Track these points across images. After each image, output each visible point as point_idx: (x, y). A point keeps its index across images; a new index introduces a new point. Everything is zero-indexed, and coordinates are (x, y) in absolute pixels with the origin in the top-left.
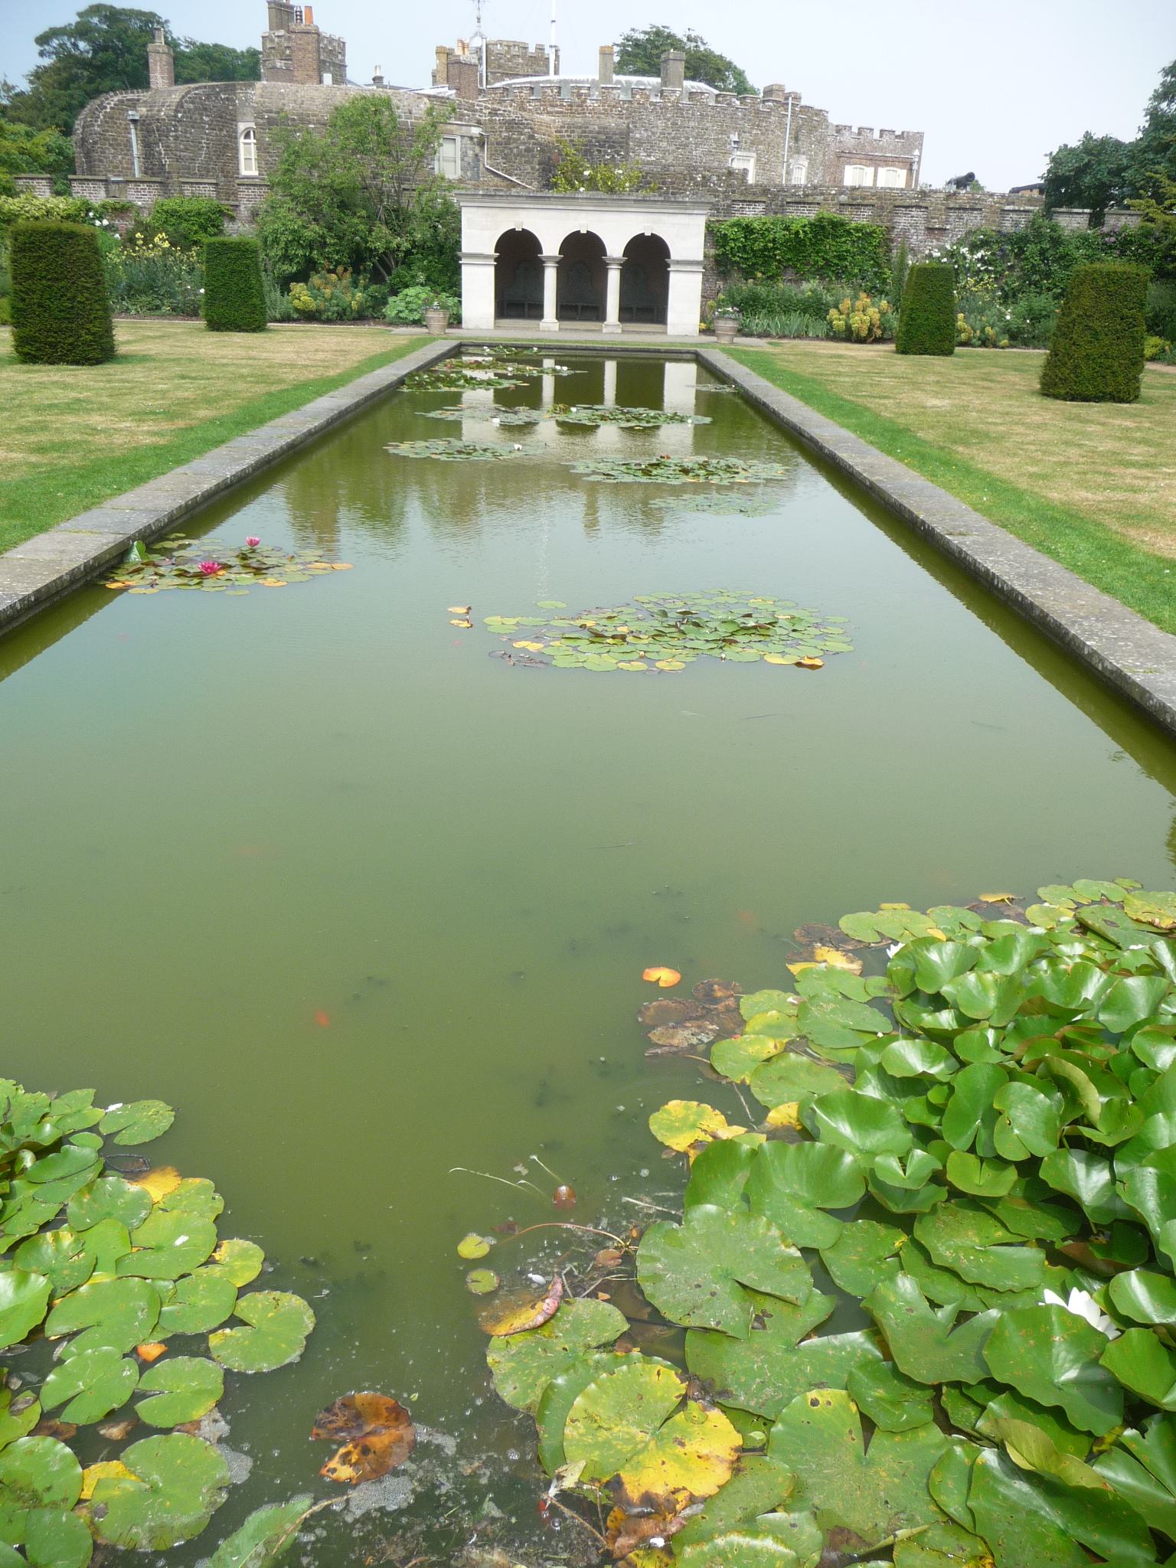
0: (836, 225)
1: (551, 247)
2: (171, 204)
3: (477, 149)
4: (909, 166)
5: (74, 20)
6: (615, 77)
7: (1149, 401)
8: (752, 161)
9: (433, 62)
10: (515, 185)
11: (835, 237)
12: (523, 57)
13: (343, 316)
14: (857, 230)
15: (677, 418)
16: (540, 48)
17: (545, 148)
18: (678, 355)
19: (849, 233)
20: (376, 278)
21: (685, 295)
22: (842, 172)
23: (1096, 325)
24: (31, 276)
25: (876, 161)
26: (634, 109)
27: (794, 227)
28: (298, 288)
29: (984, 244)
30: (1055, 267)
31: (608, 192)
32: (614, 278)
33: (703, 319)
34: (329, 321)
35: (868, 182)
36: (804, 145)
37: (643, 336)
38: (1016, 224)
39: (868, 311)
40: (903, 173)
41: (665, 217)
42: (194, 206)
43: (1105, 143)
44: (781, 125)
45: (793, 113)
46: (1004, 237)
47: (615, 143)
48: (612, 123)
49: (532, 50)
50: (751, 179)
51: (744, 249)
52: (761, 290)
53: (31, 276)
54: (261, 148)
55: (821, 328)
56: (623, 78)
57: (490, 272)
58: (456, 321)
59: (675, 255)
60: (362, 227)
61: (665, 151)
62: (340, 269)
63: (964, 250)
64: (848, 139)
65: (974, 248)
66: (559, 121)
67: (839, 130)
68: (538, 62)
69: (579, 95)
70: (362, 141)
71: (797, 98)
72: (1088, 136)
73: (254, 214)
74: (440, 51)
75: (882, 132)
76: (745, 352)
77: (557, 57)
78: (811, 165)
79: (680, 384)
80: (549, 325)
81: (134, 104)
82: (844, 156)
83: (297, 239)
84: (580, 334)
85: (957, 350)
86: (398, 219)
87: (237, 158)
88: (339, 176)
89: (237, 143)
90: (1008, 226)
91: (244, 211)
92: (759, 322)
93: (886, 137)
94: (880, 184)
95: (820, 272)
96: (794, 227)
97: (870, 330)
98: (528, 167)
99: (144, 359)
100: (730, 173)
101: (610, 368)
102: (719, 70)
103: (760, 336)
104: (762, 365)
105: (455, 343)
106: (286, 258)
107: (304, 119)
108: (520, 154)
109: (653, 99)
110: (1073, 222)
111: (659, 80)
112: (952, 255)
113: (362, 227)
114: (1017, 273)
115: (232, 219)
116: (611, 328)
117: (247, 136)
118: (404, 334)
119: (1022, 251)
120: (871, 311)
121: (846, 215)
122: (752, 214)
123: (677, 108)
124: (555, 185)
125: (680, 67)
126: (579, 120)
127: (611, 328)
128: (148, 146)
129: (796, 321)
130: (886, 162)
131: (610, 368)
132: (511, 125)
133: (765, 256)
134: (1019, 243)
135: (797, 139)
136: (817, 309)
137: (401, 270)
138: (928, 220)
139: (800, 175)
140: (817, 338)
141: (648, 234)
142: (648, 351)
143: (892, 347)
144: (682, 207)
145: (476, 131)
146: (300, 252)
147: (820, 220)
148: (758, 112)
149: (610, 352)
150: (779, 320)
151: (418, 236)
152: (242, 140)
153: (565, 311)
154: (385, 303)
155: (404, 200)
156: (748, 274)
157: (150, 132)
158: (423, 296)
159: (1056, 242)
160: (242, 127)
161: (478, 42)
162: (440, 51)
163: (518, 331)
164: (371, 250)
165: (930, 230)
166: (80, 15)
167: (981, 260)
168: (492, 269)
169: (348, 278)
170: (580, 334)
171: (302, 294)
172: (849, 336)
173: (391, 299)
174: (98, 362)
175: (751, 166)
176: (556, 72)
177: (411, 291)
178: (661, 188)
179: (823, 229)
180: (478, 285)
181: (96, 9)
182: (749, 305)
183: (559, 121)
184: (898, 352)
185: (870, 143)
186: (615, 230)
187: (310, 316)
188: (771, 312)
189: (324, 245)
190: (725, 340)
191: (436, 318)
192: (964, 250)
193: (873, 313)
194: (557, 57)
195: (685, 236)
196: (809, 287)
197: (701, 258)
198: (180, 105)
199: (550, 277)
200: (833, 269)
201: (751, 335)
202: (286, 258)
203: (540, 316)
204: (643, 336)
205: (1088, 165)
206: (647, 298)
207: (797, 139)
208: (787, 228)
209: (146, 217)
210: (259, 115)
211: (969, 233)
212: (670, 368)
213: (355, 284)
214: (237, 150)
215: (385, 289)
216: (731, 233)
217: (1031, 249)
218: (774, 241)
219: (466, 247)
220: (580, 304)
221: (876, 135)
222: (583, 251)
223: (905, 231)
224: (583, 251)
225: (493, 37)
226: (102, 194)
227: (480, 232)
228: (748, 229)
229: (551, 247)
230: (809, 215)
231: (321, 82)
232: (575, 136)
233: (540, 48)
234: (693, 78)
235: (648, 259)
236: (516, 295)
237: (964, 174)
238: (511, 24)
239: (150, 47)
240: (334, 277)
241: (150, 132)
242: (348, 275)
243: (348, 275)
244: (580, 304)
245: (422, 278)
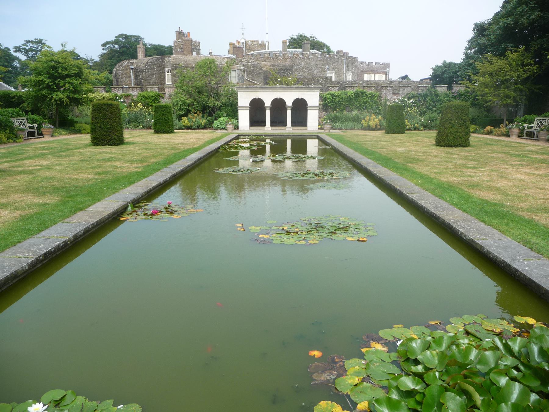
0: (362, 93)
1: (268, 103)
2: (143, 94)
3: (243, 73)
4: (386, 73)
5: (114, 39)
6: (288, 50)
7: (473, 146)
8: (333, 74)
9: (228, 47)
10: (255, 84)
11: (362, 97)
12: (257, 45)
13: (199, 127)
14: (370, 94)
15: (312, 158)
16: (263, 42)
17: (265, 72)
18: (311, 137)
19: (367, 95)
20: (210, 115)
21: (313, 118)
22: (363, 76)
23: (453, 122)
24: (98, 118)
25: (374, 73)
26: (294, 59)
27: (348, 94)
28: (184, 119)
29: (413, 97)
30: (437, 104)
31: (287, 85)
32: (289, 112)
33: (319, 124)
34: (194, 129)
35: (372, 79)
36: (350, 68)
37: (299, 131)
38: (423, 91)
39: (375, 120)
40: (384, 76)
41: (305, 93)
42: (151, 94)
43: (450, 64)
44: (343, 63)
45: (346, 58)
46: (419, 95)
47: (288, 70)
48: (287, 64)
49: (260, 42)
50: (333, 79)
51: (332, 102)
52: (339, 115)
53: (98, 118)
55: (359, 126)
56: (290, 50)
57: (247, 112)
58: (237, 128)
59: (309, 104)
60: (205, 99)
61: (304, 72)
62: (198, 112)
63: (406, 99)
64: (365, 66)
65: (409, 99)
66: (269, 64)
67: (362, 63)
68: (262, 46)
69: (276, 56)
70: (205, 72)
71: (347, 54)
72: (445, 62)
73: (170, 96)
74: (230, 44)
75: (376, 63)
76: (334, 135)
77: (268, 44)
78: (353, 74)
79: (312, 146)
80: (268, 128)
81: (132, 64)
82: (364, 71)
83: (184, 103)
84: (278, 131)
85: (406, 132)
86: (217, 96)
87: (165, 79)
88: (198, 83)
89: (165, 74)
90: (420, 91)
91: (167, 95)
92: (338, 125)
93: (377, 65)
94: (376, 79)
95: (358, 108)
96: (348, 94)
97: (376, 126)
98: (260, 78)
99: (133, 143)
100: (326, 78)
101: (289, 142)
102: (321, 46)
103: (339, 129)
104: (339, 139)
105: (236, 135)
106: (180, 109)
107: (187, 66)
108: (257, 74)
109: (300, 56)
110: (442, 89)
111: (301, 50)
112: (402, 101)
113: (205, 99)
114: (424, 106)
115: (163, 98)
116: (289, 129)
117: (168, 72)
118: (219, 133)
119: (425, 99)
120: (376, 120)
121: (366, 90)
122: (334, 90)
123: (308, 59)
124: (269, 83)
125: (309, 46)
126: (276, 63)
128: (136, 76)
129: (350, 124)
130: (378, 73)
131: (289, 142)
132: (254, 66)
133: (339, 104)
134: (424, 96)
135: (348, 66)
136: (357, 120)
137: (218, 112)
138: (393, 90)
139: (350, 77)
140: (358, 129)
141: (300, 98)
142: (301, 135)
143: (384, 131)
144: (311, 89)
145: (242, 68)
146: (185, 107)
147: (357, 91)
148: (335, 59)
149: (288, 136)
150: (345, 124)
151: (224, 101)
152: (167, 73)
153: (273, 124)
154: (213, 123)
155: (219, 90)
156: (334, 109)
157: (137, 72)
158: (226, 120)
159: (437, 96)
160: (167, 69)
161: (242, 41)
162: (231, 44)
163: (257, 130)
164: (208, 106)
165: (394, 93)
166: (116, 37)
167: (412, 102)
168: (248, 111)
169: (201, 115)
170: (278, 131)
171: (185, 121)
172: (369, 128)
173: (215, 121)
174: (118, 145)
175: (333, 75)
176: (268, 49)
177: (222, 119)
178: (305, 83)
179: (358, 95)
180: (244, 117)
181: (121, 35)
182: (334, 120)
183: (269, 64)
184: (386, 133)
185: (372, 67)
187: (188, 128)
188: (342, 122)
189: (193, 105)
190: (327, 131)
191: (230, 127)
192: (406, 99)
193: (377, 120)
194: (268, 44)
195: (312, 98)
196: (355, 113)
197: (318, 105)
198: (147, 63)
200: (362, 107)
201: (336, 129)
202: (180, 109)
204: (299, 131)
205: (445, 71)
206: (300, 118)
207: (348, 66)
208: (346, 95)
209: (135, 98)
210: (172, 65)
211: (407, 94)
212: (309, 141)
213: (203, 117)
214: (165, 76)
215: (213, 118)
216: (328, 96)
217: (429, 98)
218: (342, 99)
219: (239, 105)
220: (278, 120)
221: (374, 64)
222: (279, 105)
223: (386, 94)
224: (279, 105)
225: (247, 39)
226: (121, 91)
227: (244, 99)
228: (333, 95)
229: (268, 103)
230: (354, 90)
231: (192, 55)
232: (275, 68)
234: (313, 49)
235: (300, 106)
236: (257, 119)
237: (404, 75)
238: (253, 34)
239: (138, 46)
240: (196, 115)
241: (137, 72)
242: (201, 114)
243: (201, 114)
244: (278, 120)
245: (225, 114)
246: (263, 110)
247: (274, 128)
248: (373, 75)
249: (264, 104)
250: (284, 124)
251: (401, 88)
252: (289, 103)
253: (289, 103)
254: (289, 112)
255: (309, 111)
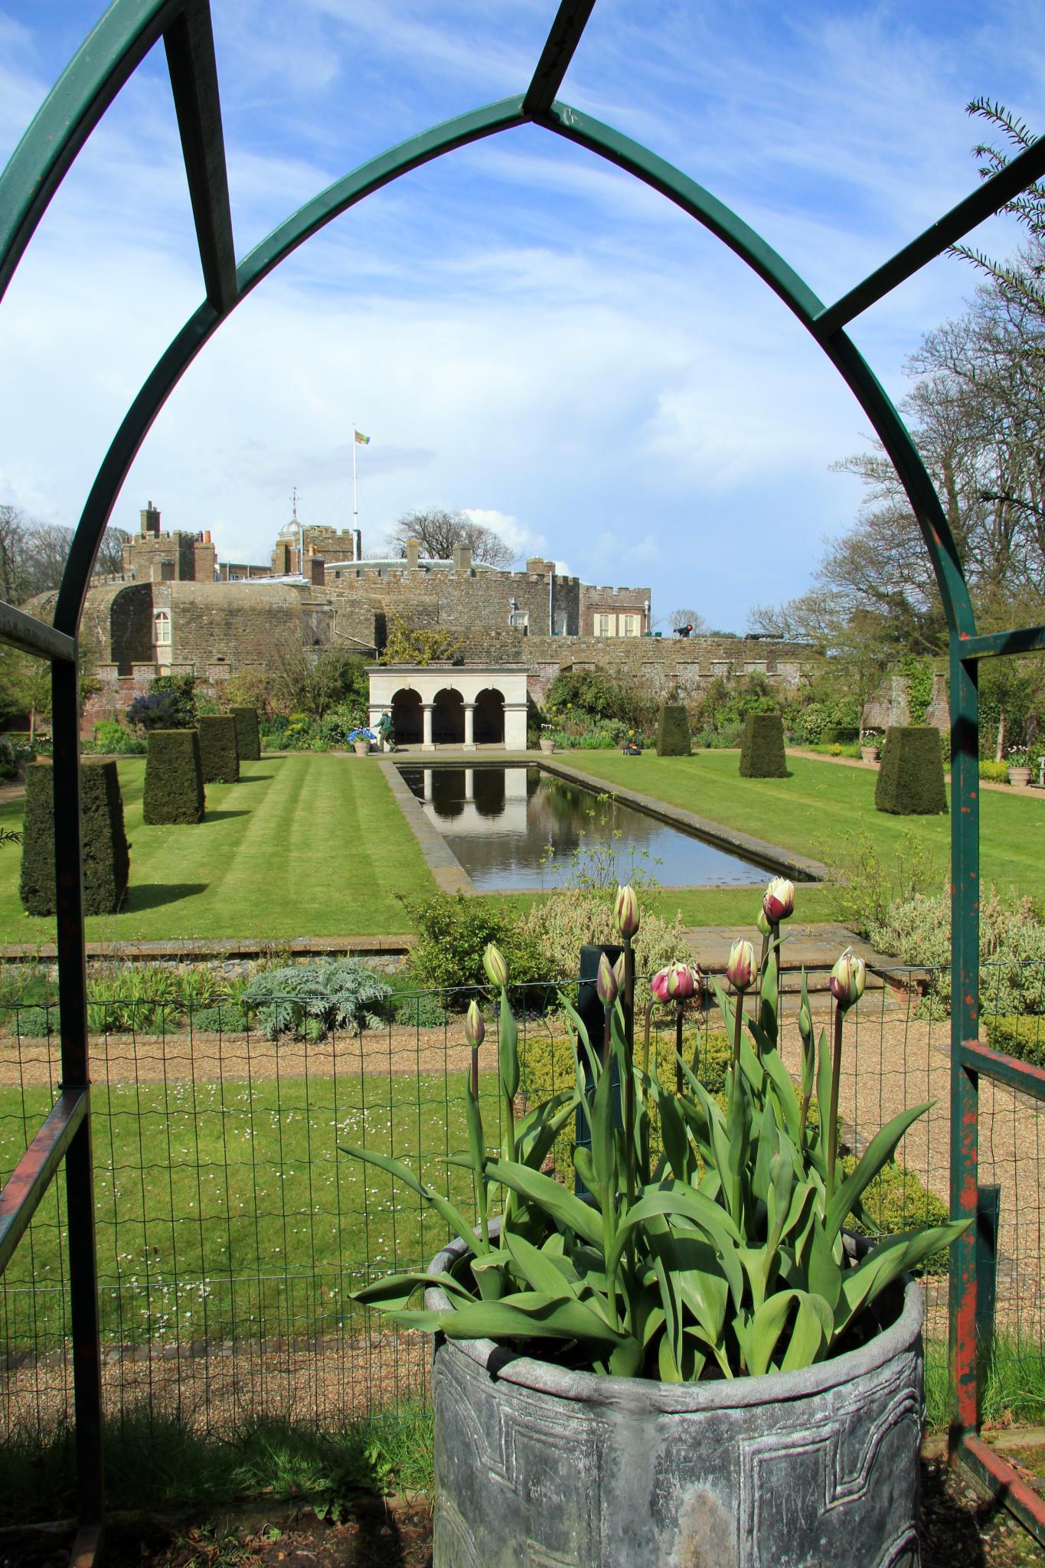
12: (332, 538)
16: (346, 532)
21: (515, 724)
25: (616, 610)
32: (469, 716)
37: (489, 752)
40: (637, 619)
49: (339, 533)
54: (176, 627)
59: (507, 701)
67: (588, 589)
79: (515, 782)
80: (427, 748)
82: (593, 607)
84: (450, 752)
101: (469, 774)
107: (209, 608)
108: (360, 622)
116: (468, 748)
127: (468, 748)
131: (469, 774)
153: (437, 738)
160: (155, 611)
161: (294, 528)
170: (450, 752)
186: (470, 687)
199: (427, 716)
203: (422, 741)
204: (489, 752)
206: (490, 728)
210: (174, 607)
212: (508, 771)
219: (372, 701)
220: (448, 732)
221: (615, 589)
222: (449, 700)
224: (449, 700)
225: (307, 521)
227: (382, 690)
229: (428, 698)
232: (400, 609)
233: (346, 532)
235: (491, 705)
244: (448, 732)
246: (421, 709)
247: (440, 746)
248: (612, 618)
249: (420, 699)
250: (463, 740)
251: (681, 667)
252: (470, 698)
253: (470, 698)
254: (469, 716)
255: (507, 714)
